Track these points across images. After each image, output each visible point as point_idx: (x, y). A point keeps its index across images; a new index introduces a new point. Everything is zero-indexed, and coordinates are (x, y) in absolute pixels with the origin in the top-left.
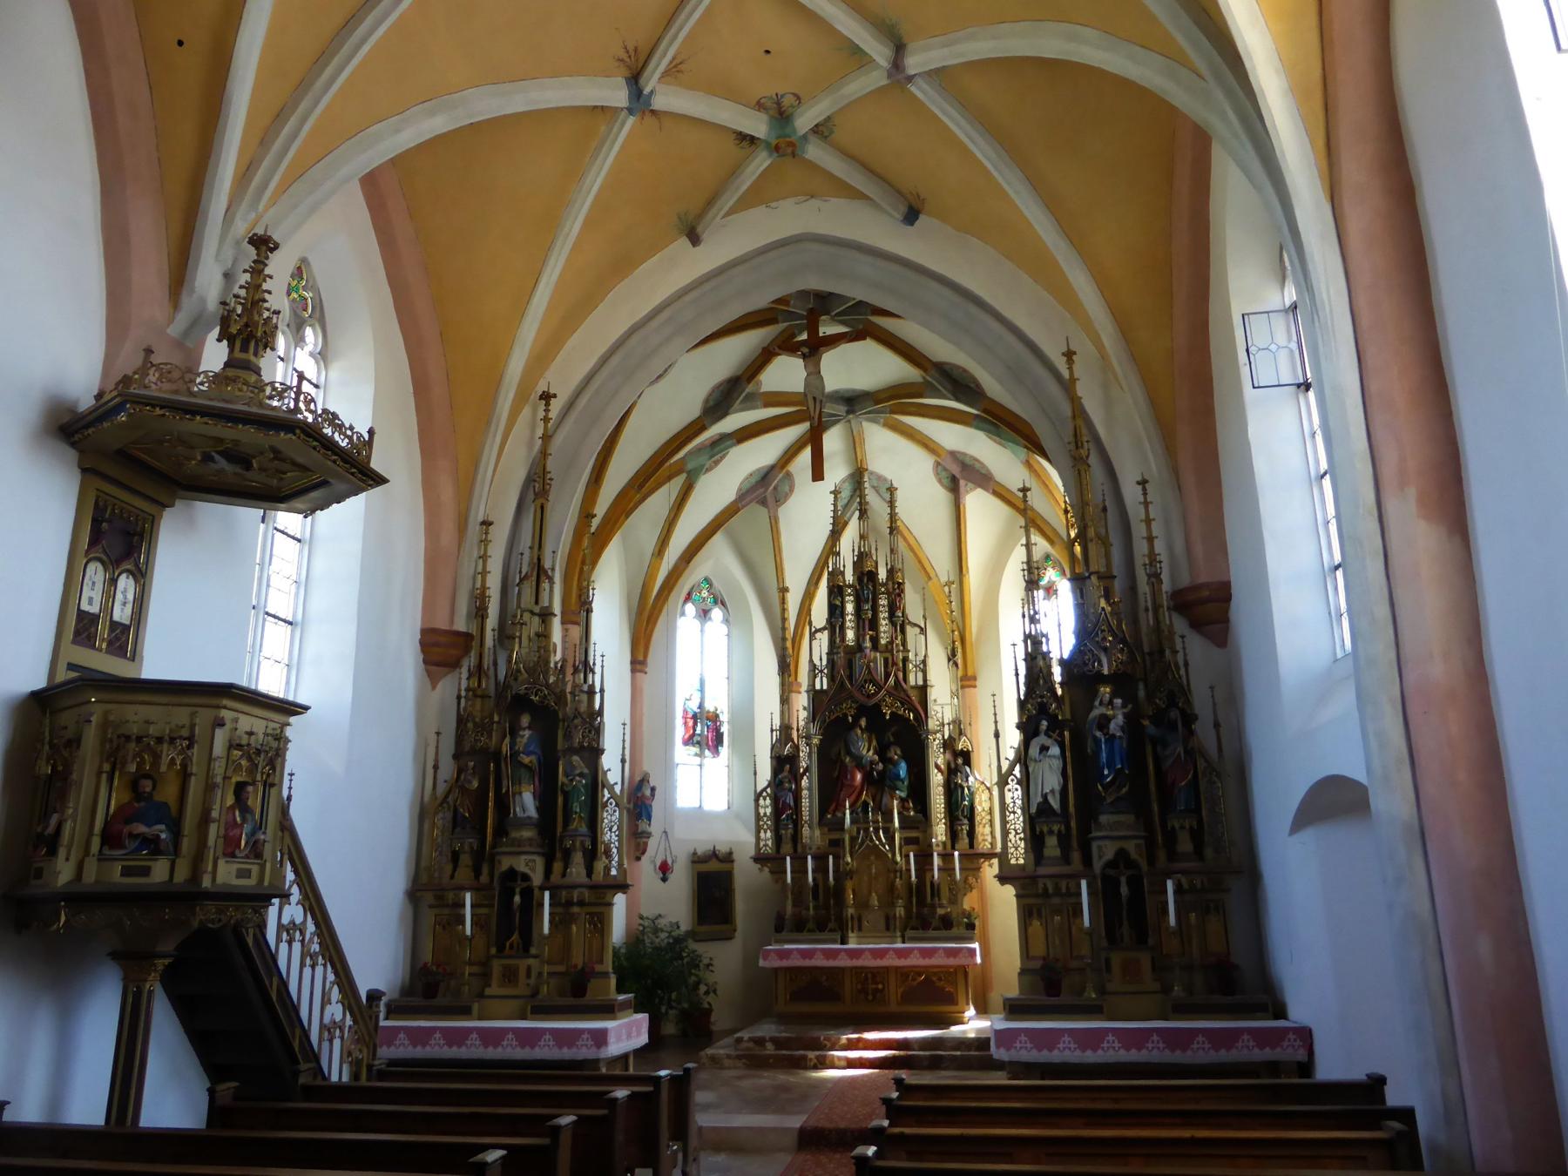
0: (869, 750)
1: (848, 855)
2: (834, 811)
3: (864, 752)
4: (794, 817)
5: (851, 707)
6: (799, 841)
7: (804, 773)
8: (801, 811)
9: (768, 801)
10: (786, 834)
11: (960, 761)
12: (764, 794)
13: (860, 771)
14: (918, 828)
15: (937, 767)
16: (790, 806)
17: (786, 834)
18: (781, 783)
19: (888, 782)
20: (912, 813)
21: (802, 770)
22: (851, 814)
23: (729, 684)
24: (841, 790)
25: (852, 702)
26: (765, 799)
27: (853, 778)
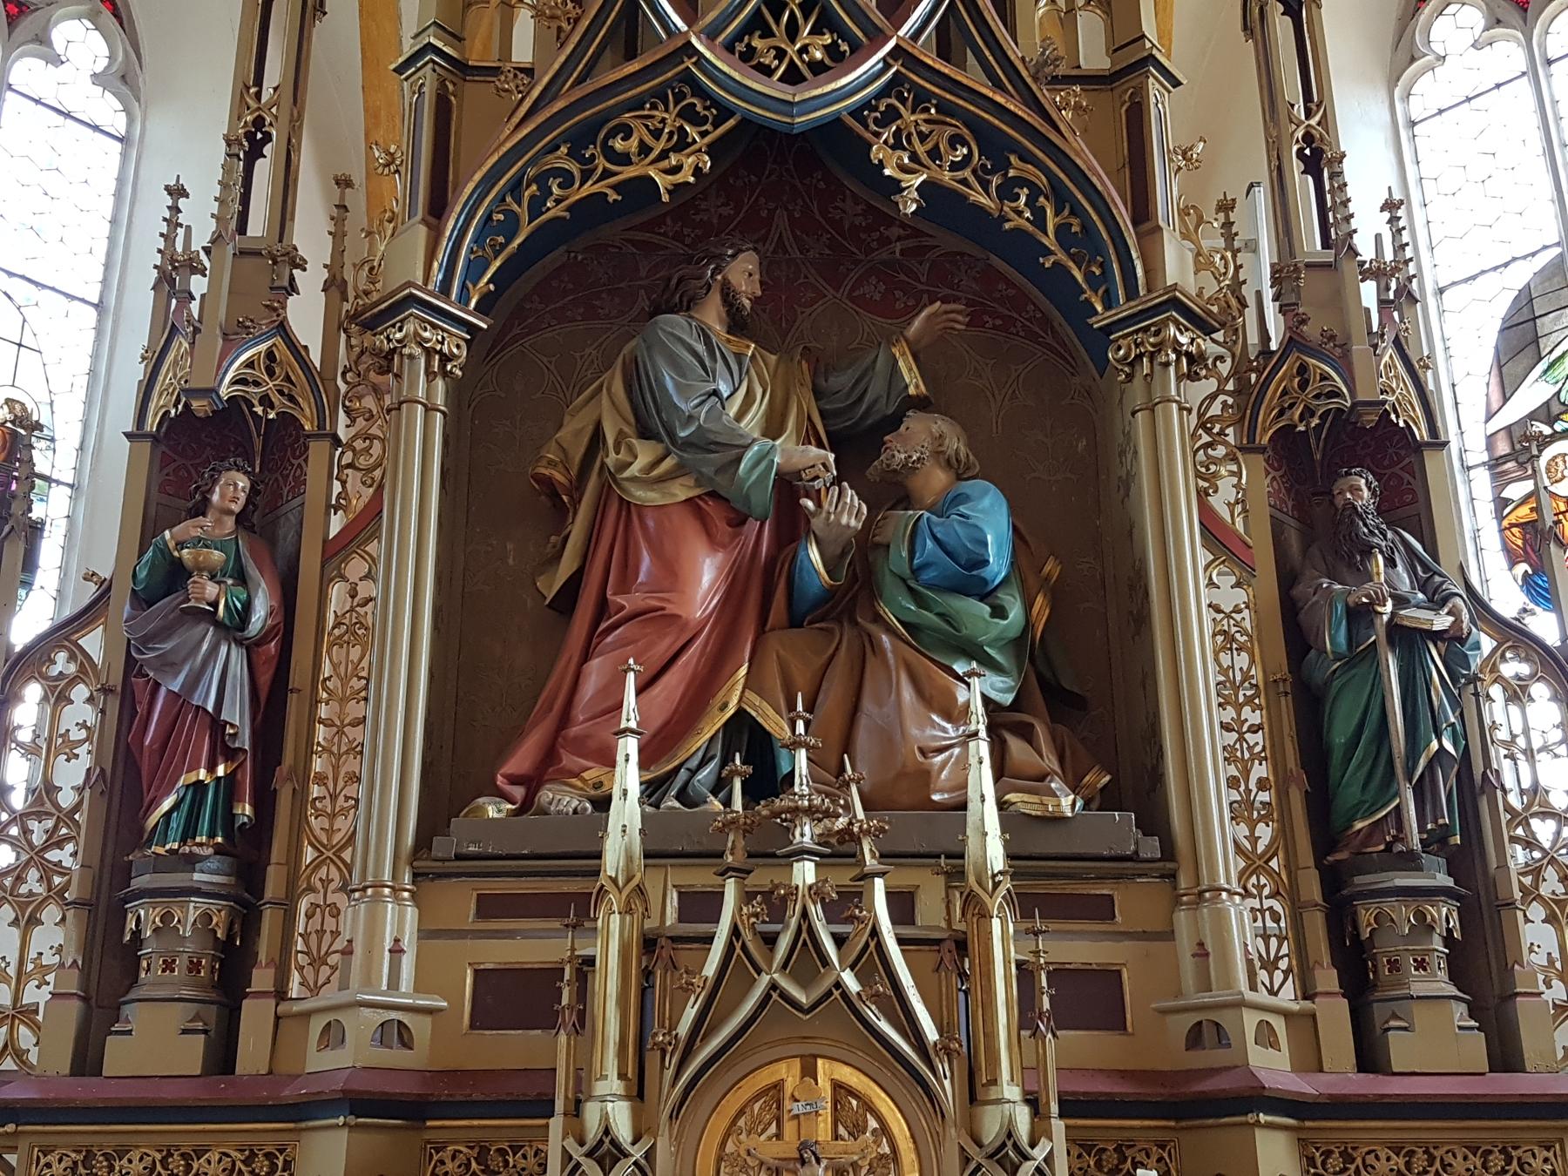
0: (773, 428)
1: (610, 1084)
2: (532, 783)
3: (751, 424)
4: (245, 810)
5: (682, 144)
6: (262, 978)
7: (336, 552)
8: (303, 776)
9: (80, 711)
10: (166, 926)
11: (1362, 490)
12: (61, 663)
13: (714, 543)
14: (1102, 909)
15: (1214, 533)
16: (216, 725)
17: (166, 926)
18: (173, 576)
19: (896, 606)
20: (1067, 803)
21: (336, 524)
22: (653, 790)
23: (99, 330)
24: (586, 657)
25: (689, 114)
26: (58, 696)
27: (672, 574)
